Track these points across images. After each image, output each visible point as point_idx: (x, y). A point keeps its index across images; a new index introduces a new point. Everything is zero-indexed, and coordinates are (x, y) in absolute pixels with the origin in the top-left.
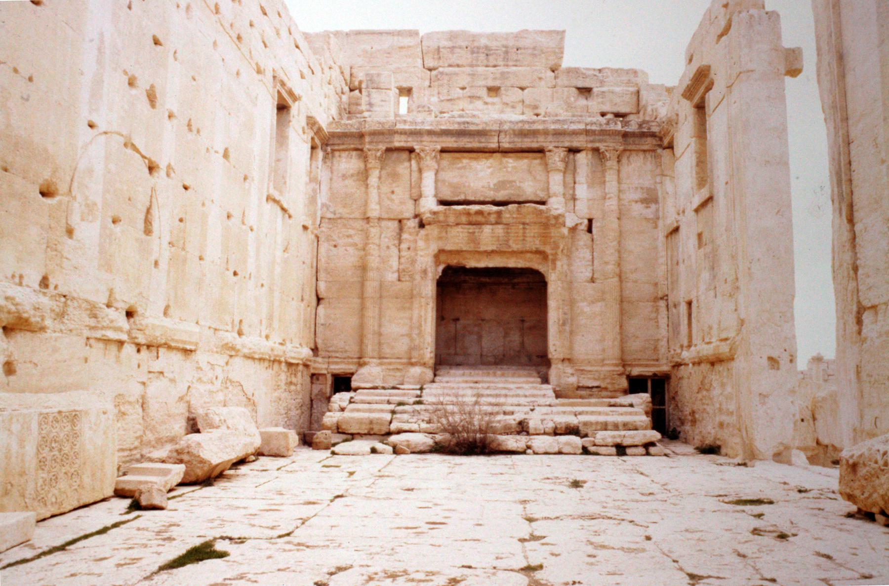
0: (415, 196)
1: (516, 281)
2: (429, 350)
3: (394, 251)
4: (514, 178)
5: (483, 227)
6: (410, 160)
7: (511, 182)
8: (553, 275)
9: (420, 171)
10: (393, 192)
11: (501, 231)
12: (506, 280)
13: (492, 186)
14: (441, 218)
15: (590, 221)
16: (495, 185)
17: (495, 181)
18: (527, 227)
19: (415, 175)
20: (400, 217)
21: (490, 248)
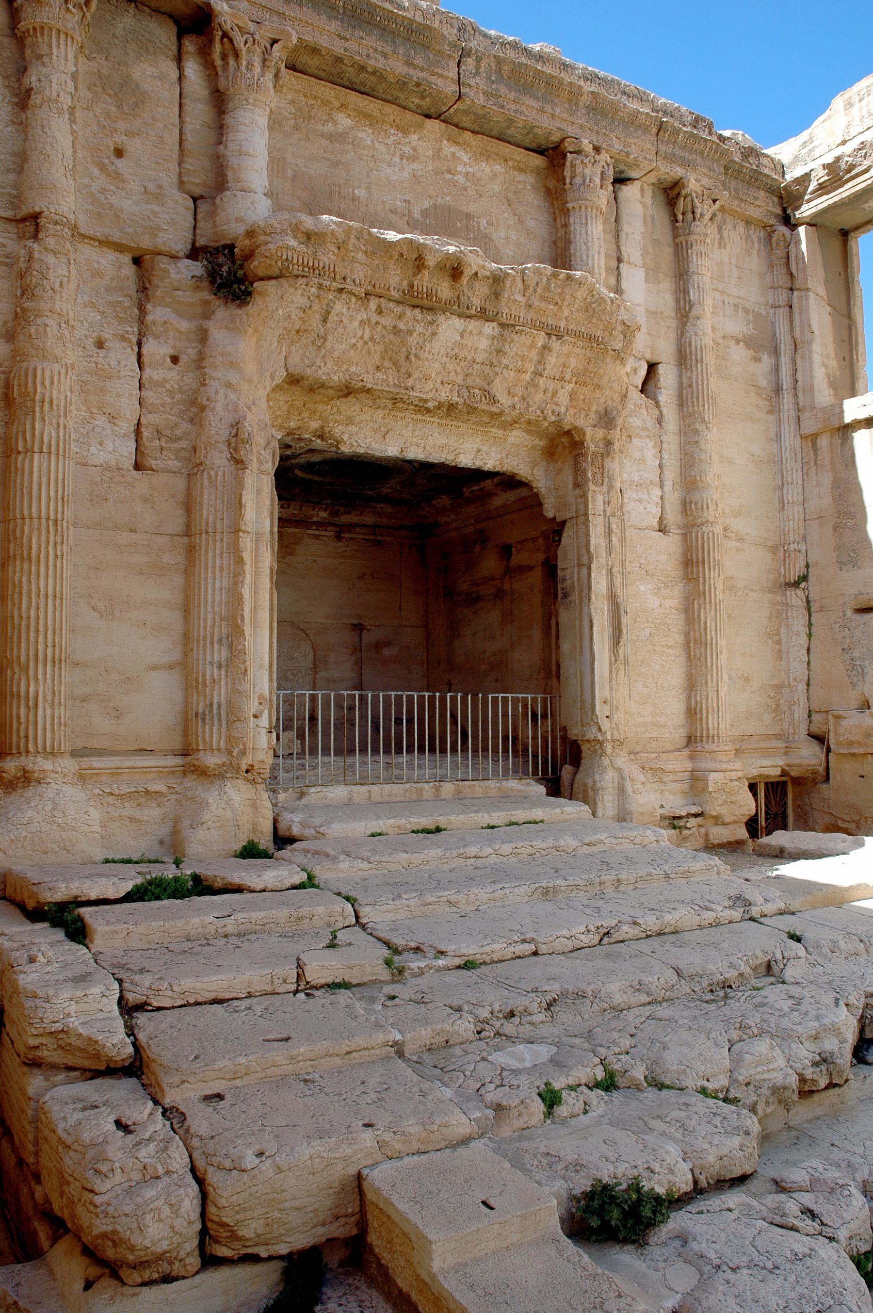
0: (197, 182)
1: (345, 519)
2: (264, 721)
3: (122, 357)
4: (472, 208)
5: (441, 319)
6: (179, 59)
7: (469, 216)
8: (600, 498)
9: (220, 102)
10: (119, 153)
11: (484, 344)
12: (324, 514)
13: (417, 215)
14: (327, 257)
15: (652, 367)
16: (425, 213)
17: (426, 204)
18: (555, 344)
19: (199, 112)
20: (146, 243)
21: (445, 394)
